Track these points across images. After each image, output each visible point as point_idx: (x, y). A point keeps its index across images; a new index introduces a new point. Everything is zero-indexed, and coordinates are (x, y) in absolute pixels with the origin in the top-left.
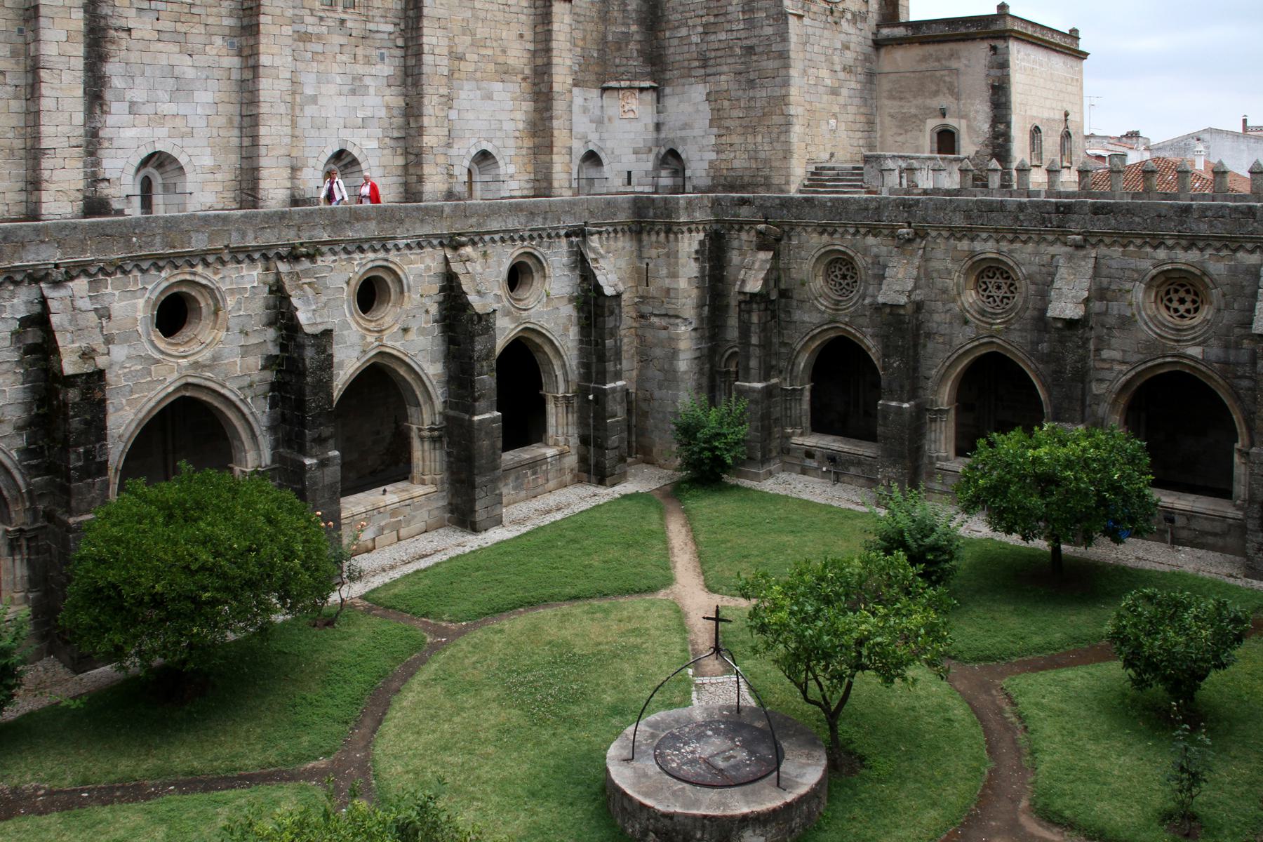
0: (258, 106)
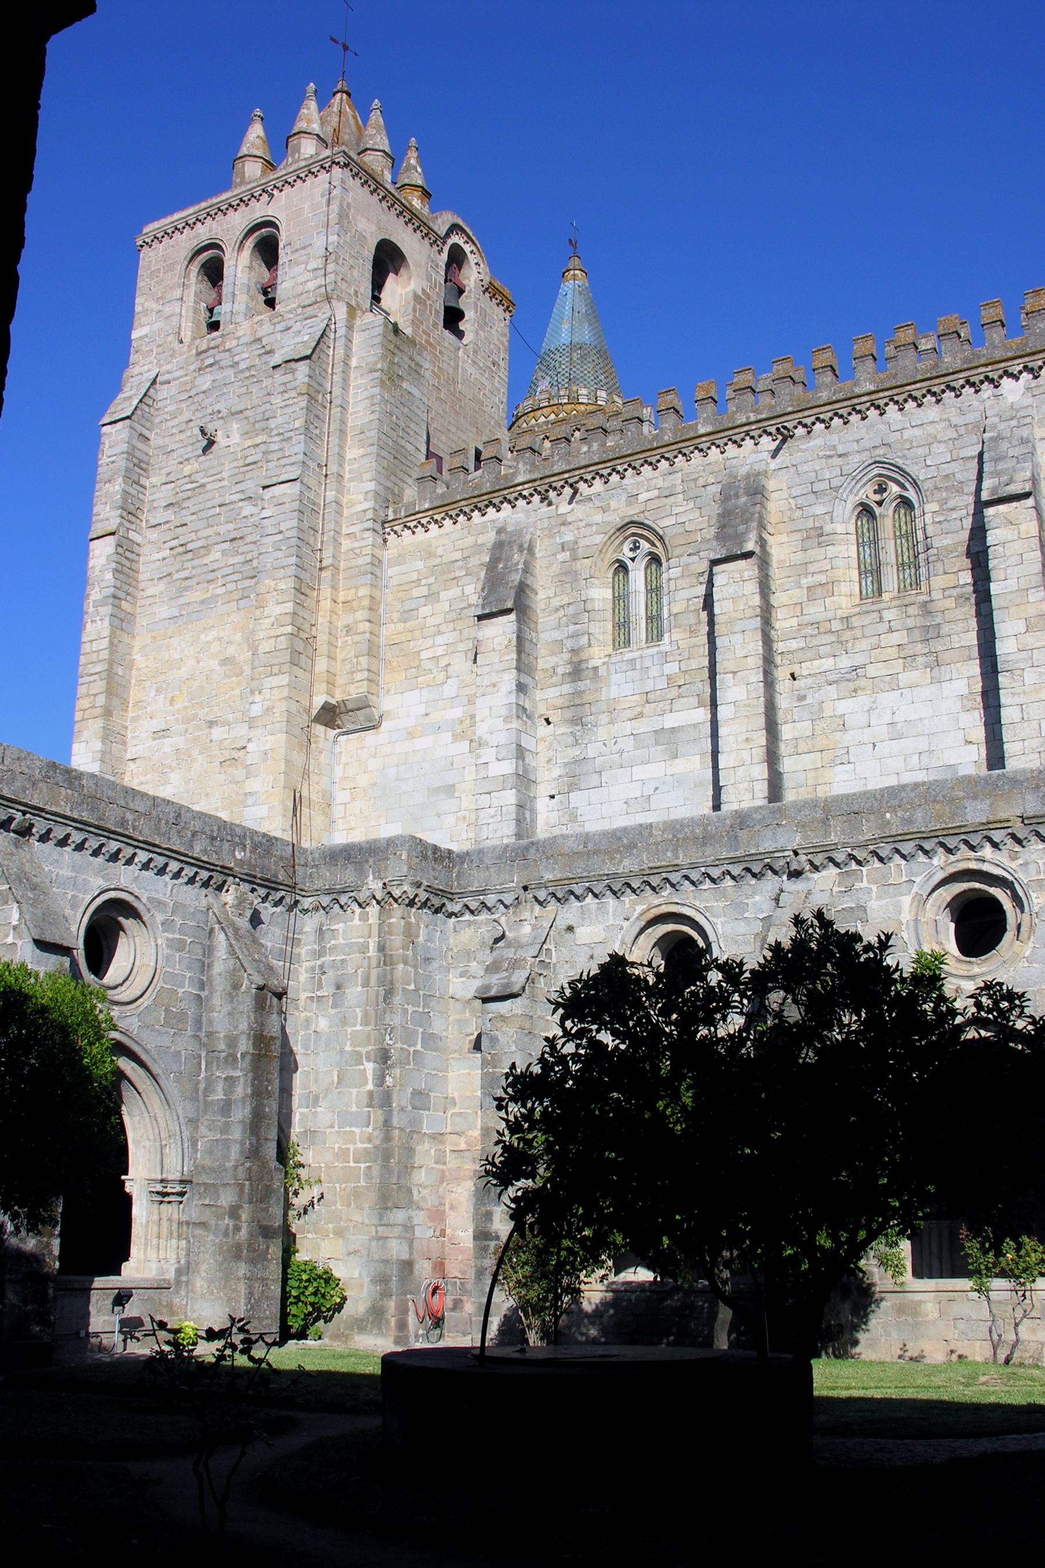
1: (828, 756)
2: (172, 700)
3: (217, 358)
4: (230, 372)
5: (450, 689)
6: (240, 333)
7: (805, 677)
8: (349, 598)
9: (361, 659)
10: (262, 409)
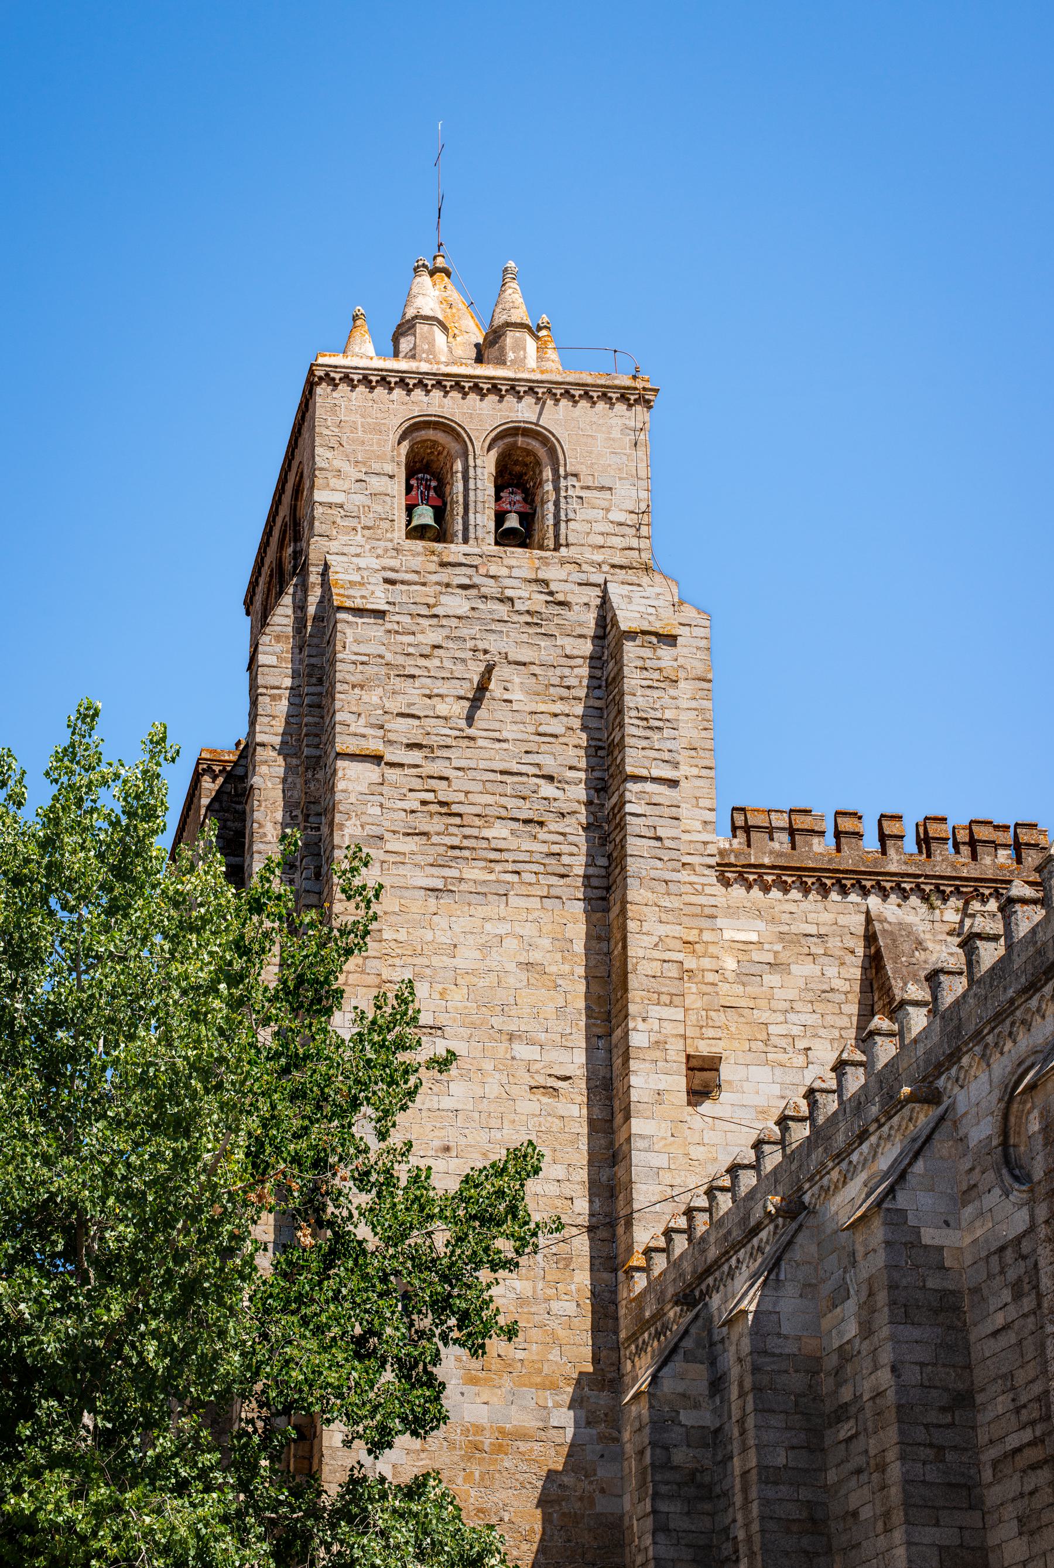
3: (477, 580)
4: (502, 610)
8: (690, 939)
10: (558, 672)
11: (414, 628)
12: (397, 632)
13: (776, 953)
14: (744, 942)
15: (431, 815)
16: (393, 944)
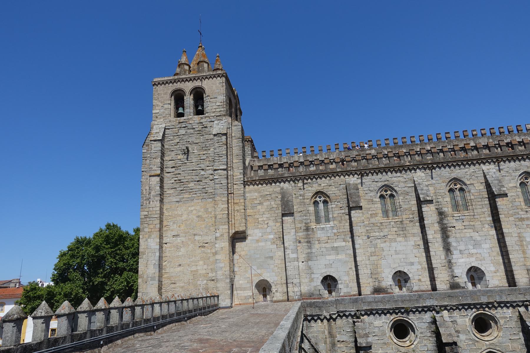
0: (507, 248)
1: (379, 257)
2: (179, 226)
3: (187, 125)
4: (192, 131)
5: (269, 230)
6: (195, 119)
7: (372, 237)
8: (238, 202)
9: (243, 220)
10: (205, 144)
11: (173, 139)
12: (169, 141)
13: (260, 200)
14: (253, 199)
15: (177, 183)
16: (169, 216)
